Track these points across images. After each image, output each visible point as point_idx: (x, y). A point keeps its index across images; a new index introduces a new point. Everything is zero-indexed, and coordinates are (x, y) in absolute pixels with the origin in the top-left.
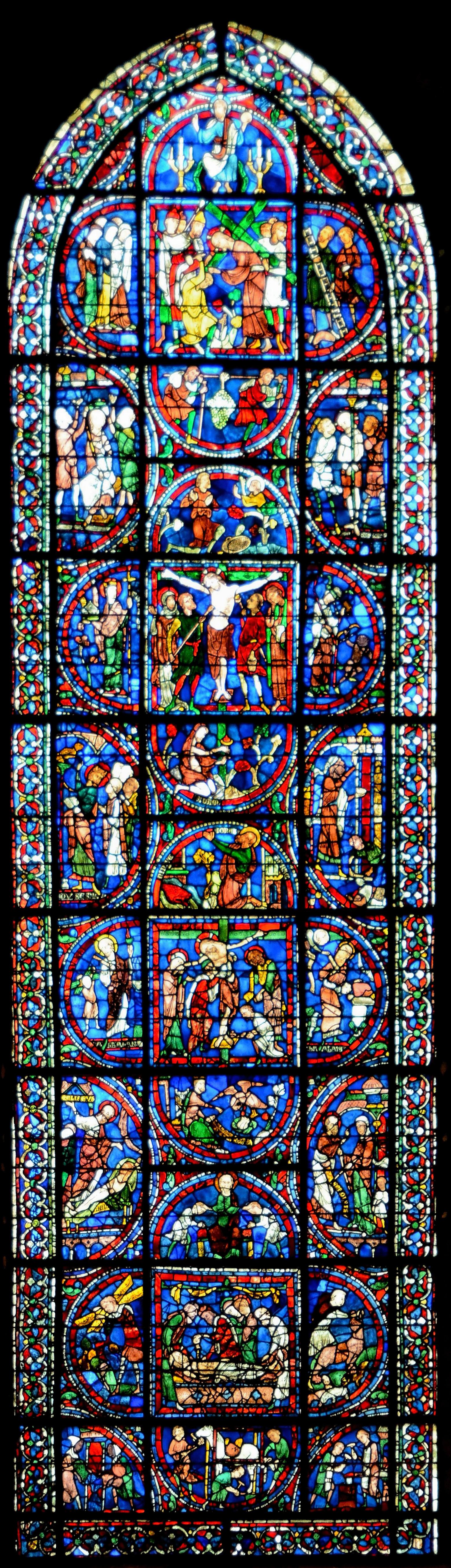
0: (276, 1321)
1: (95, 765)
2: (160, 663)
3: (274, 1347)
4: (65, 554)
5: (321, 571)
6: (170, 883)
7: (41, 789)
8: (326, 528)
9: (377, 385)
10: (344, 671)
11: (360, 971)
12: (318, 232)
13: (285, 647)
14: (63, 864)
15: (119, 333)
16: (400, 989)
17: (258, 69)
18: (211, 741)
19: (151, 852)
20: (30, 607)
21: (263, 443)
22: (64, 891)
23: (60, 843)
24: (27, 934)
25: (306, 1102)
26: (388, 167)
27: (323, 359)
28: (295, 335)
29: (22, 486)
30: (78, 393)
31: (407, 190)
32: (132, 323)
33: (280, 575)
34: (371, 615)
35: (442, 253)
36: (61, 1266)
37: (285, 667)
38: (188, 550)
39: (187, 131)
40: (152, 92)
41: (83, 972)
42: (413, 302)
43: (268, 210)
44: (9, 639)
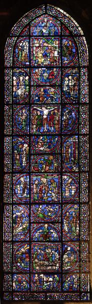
0: (56, 253)
4: (15, 104)
8: (66, 98)
12: (65, 42)
13: (58, 121)
18: (43, 139)
19: (31, 161)
23: (13, 159)
25: (62, 210)
29: (6, 91)
31: (82, 34)
36: (13, 242)
41: (18, 184)
44: (4, 120)
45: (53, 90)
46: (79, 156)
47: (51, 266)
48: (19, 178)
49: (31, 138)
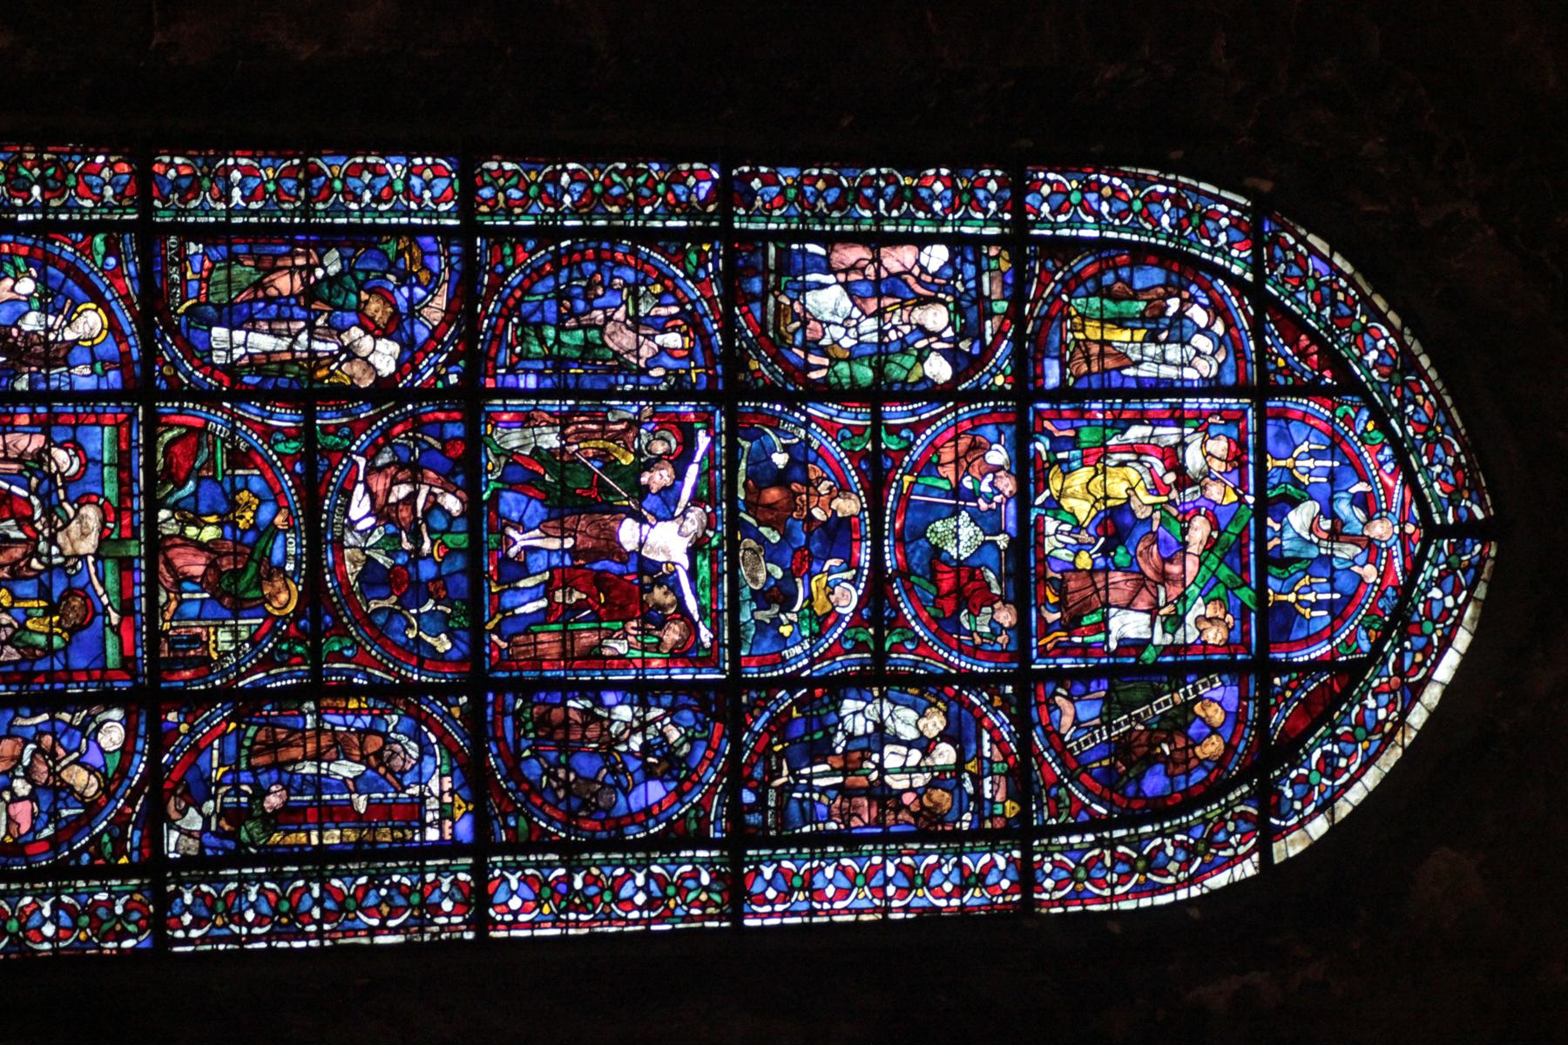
1: (395, 306)
2: (564, 427)
5: (714, 720)
6: (199, 446)
7: (354, 206)
8: (780, 724)
9: (999, 811)
10: (559, 765)
11: (54, 815)
13: (594, 656)
14: (229, 245)
15: (1061, 358)
16: (22, 893)
17: (1436, 593)
18: (439, 522)
19: (252, 411)
20: (646, 192)
21: (907, 611)
22: (182, 246)
23: (261, 240)
24: (106, 173)
26: (1311, 818)
27: (1034, 713)
28: (1067, 663)
29: (832, 182)
30: (972, 284)
32: (1077, 378)
33: (708, 644)
34: (647, 811)
35: (1194, 913)
37: (563, 655)
38: (742, 478)
39: (1348, 473)
40: (1400, 413)
42: (1121, 868)
43: (1244, 612)
45: (848, 600)
46: (301, 855)
48: (102, 303)
49: (443, 416)
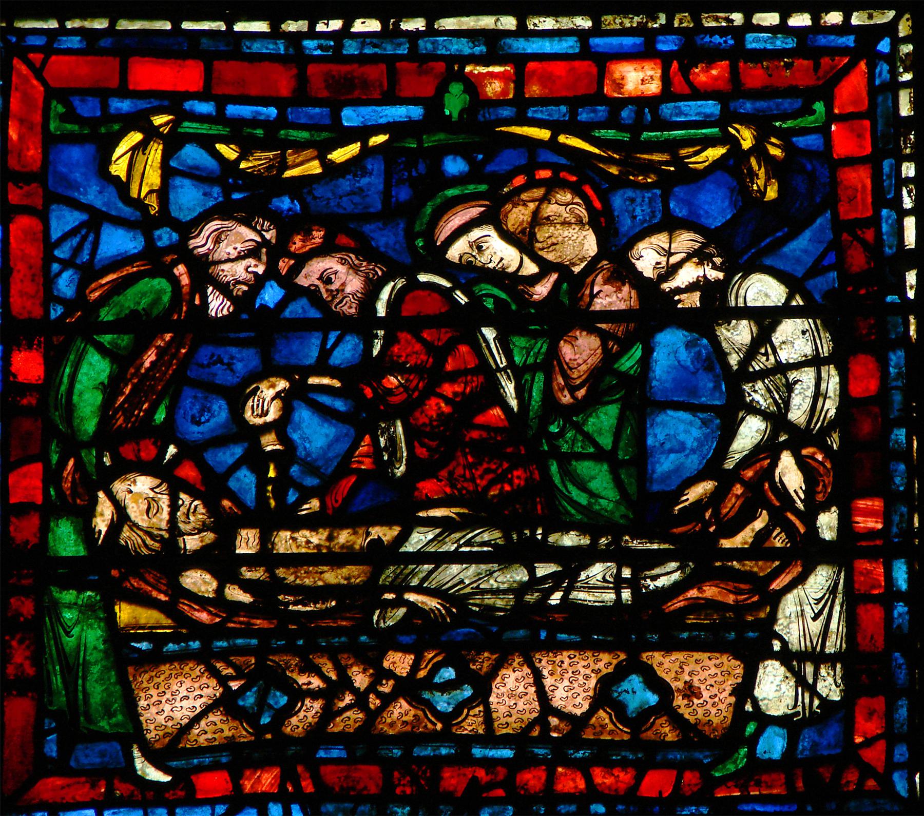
3: (751, 431)
47: (586, 629)
